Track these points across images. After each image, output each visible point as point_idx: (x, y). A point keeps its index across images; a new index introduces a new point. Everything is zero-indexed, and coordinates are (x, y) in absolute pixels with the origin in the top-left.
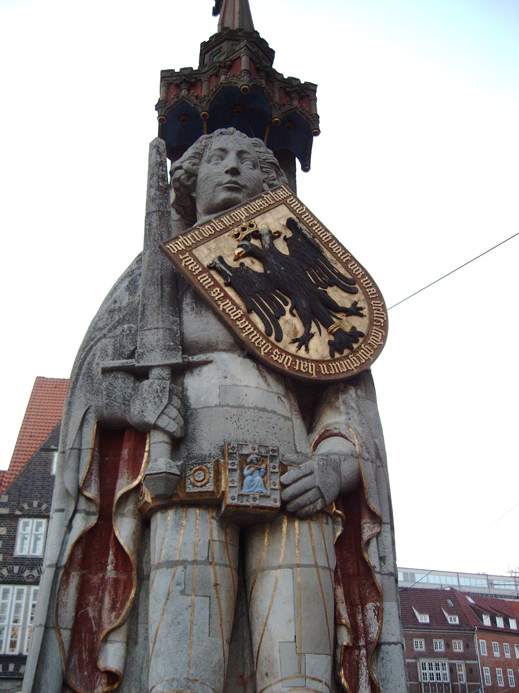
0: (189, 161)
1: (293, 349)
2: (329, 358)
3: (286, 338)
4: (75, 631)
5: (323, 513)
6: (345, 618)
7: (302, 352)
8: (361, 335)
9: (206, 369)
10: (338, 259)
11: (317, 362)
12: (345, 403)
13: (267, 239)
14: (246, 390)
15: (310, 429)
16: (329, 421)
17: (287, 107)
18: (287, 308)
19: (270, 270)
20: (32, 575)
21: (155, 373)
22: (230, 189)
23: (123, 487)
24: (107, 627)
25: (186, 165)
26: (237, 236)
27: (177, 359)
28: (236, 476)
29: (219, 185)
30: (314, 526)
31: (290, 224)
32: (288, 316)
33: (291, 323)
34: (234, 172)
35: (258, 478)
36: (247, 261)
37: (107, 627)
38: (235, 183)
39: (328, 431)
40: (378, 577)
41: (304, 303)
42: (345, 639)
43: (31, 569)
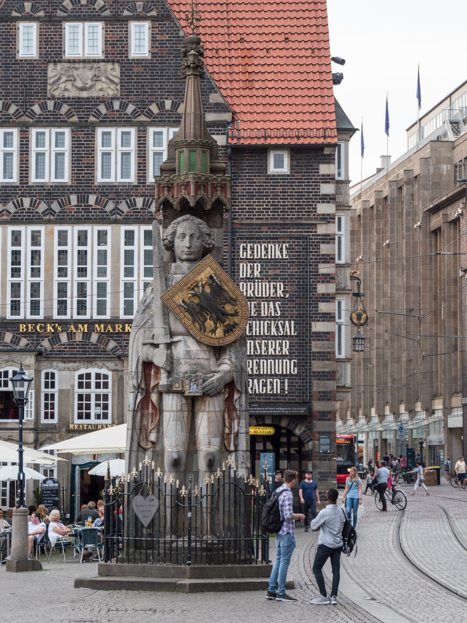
1: (210, 334)
3: (207, 330)
4: (141, 429)
5: (218, 393)
6: (227, 424)
7: (213, 336)
8: (237, 324)
10: (230, 289)
12: (230, 351)
13: (201, 288)
15: (217, 359)
17: (215, 198)
20: (7, 211)
21: (161, 346)
23: (152, 384)
24: (150, 428)
27: (169, 341)
28: (188, 386)
29: (183, 251)
30: (215, 399)
31: (211, 277)
32: (209, 321)
34: (189, 248)
35: (195, 386)
36: (193, 299)
37: (150, 428)
40: (238, 412)
41: (214, 316)
42: (227, 431)
43: (5, 202)
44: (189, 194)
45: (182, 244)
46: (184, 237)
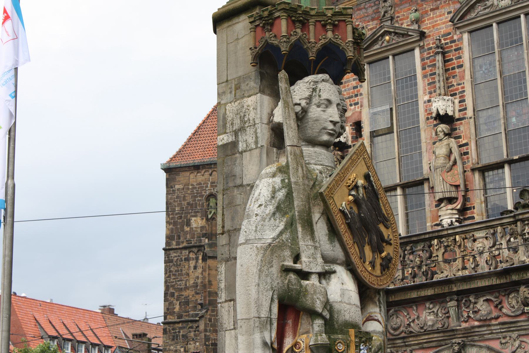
0: (305, 101)
2: (380, 275)
8: (391, 258)
9: (333, 276)
11: (377, 276)
14: (351, 292)
16: (371, 311)
18: (367, 239)
19: (363, 214)
22: (330, 134)
25: (303, 103)
26: (349, 186)
29: (325, 128)
31: (367, 177)
33: (367, 250)
38: (334, 131)
39: (371, 316)
44: (344, 39)
45: (324, 116)
46: (327, 107)
